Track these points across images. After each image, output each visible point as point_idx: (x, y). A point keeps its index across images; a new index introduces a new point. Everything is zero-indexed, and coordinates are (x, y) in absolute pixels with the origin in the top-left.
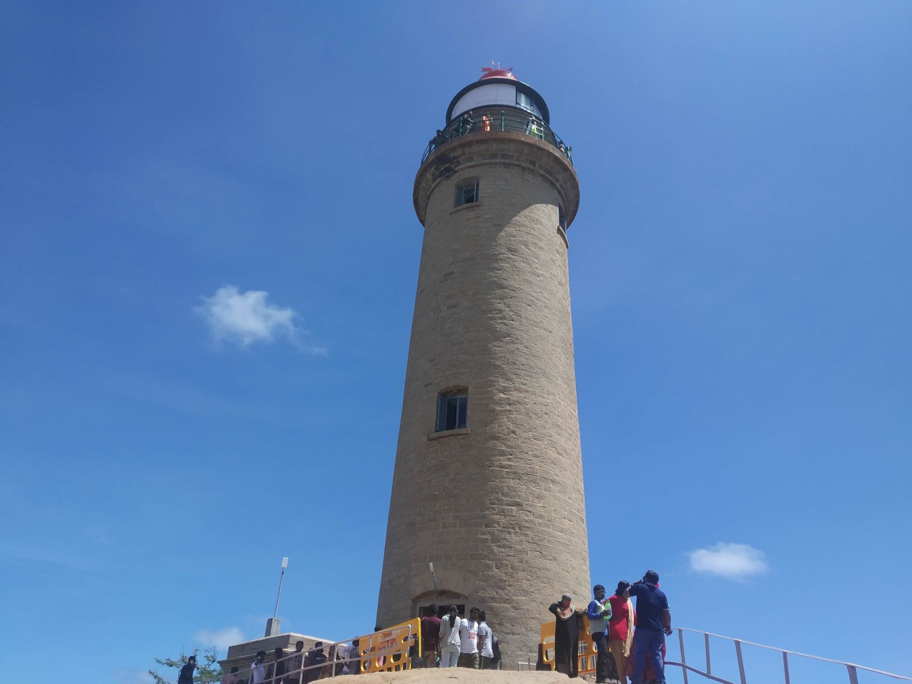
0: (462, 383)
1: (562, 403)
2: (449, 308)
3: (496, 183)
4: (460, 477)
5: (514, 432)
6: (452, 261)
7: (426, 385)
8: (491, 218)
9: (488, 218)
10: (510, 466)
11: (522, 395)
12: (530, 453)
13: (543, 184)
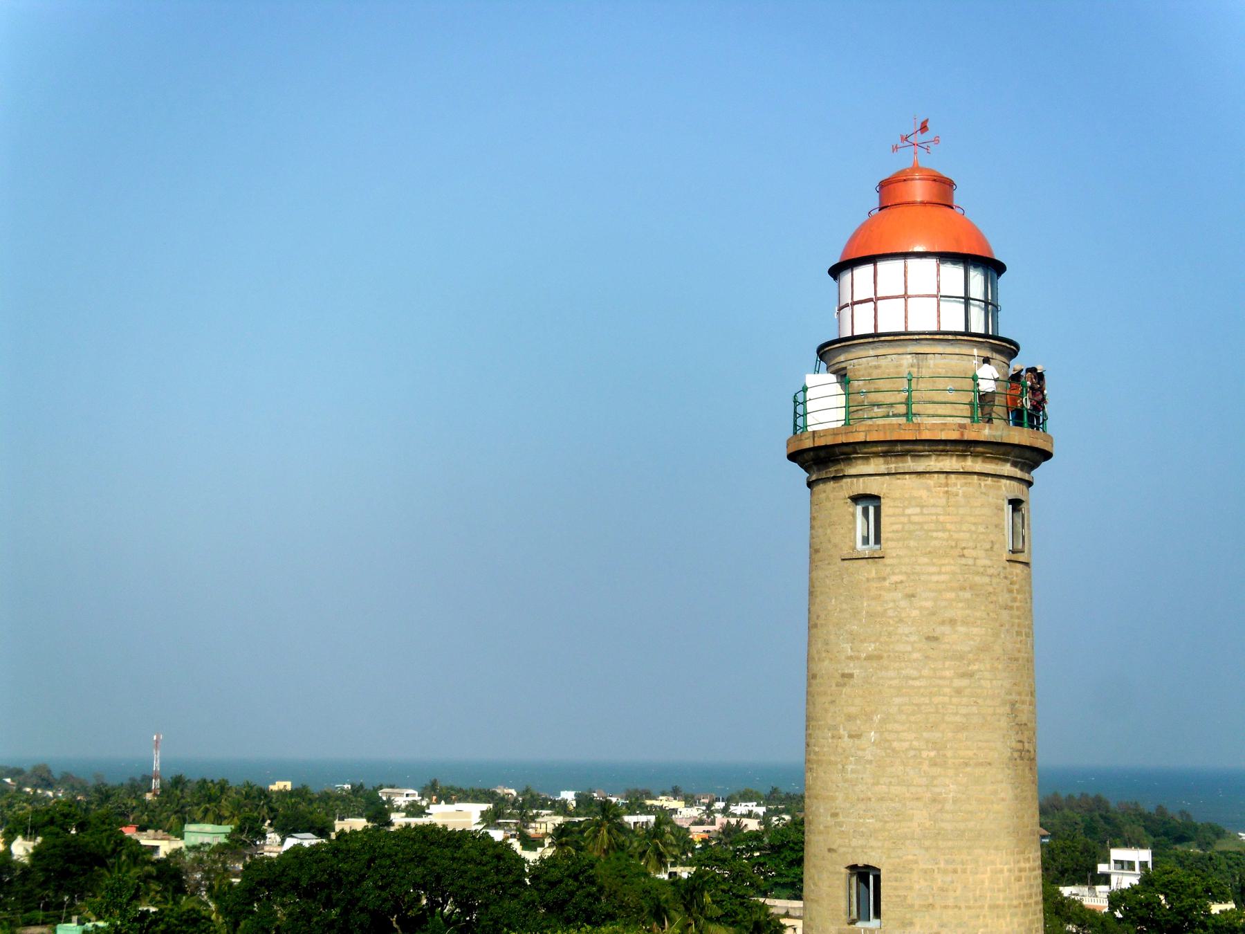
1: (1006, 867)
2: (850, 736)
3: (908, 511)
6: (850, 653)
7: (830, 850)
8: (902, 582)
9: (896, 583)
11: (948, 879)
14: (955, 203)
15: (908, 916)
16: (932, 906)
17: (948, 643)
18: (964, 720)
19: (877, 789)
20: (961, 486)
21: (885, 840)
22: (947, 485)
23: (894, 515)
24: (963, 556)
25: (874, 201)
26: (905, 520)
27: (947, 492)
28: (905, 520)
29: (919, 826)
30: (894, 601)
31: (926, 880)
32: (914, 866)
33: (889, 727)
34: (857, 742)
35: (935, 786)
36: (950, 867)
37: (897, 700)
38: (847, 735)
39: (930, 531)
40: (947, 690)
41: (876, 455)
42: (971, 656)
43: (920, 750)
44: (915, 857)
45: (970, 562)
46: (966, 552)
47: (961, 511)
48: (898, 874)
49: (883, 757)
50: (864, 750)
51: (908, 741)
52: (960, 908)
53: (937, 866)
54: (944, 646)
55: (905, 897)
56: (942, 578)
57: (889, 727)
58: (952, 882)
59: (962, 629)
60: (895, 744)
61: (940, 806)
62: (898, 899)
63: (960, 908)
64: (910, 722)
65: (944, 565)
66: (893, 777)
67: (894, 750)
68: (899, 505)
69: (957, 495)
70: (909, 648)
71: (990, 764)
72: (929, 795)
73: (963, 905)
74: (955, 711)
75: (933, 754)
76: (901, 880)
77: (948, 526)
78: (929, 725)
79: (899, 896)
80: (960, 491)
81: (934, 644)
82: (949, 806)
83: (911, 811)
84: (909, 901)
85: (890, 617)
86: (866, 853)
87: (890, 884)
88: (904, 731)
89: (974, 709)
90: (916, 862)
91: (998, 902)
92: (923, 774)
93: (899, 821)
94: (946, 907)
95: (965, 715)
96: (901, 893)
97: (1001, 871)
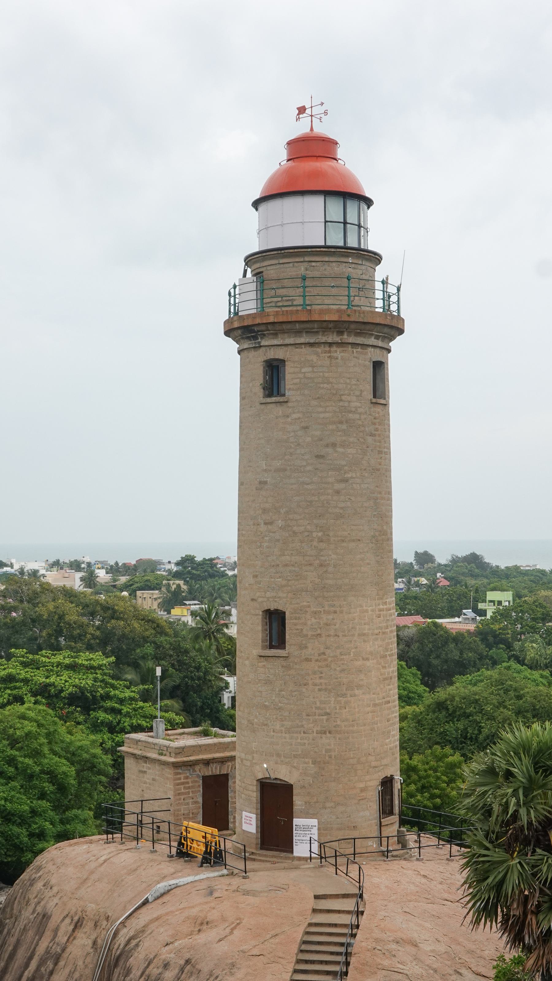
0: (280, 608)
2: (266, 524)
4: (283, 693)
5: (324, 654)
8: (299, 418)
9: (296, 419)
10: (321, 684)
11: (331, 617)
12: (338, 669)
13: (353, 351)
14: (339, 156)
15: (304, 642)
16: (320, 635)
17: (331, 460)
18: (341, 511)
19: (283, 558)
20: (340, 353)
21: (289, 592)
22: (330, 352)
23: (294, 373)
24: (341, 400)
25: (283, 155)
26: (301, 376)
27: (329, 357)
28: (301, 376)
29: (311, 582)
30: (294, 431)
31: (315, 618)
32: (308, 609)
33: (291, 516)
34: (270, 527)
35: (322, 556)
36: (332, 609)
37: (296, 498)
38: (263, 523)
39: (319, 383)
40: (330, 491)
41: (283, 332)
42: (346, 468)
43: (311, 532)
44: (308, 604)
45: (346, 404)
46: (343, 398)
47: (340, 370)
48: (297, 615)
49: (287, 537)
50: (274, 532)
51: (304, 526)
52: (339, 636)
53: (323, 609)
54: (328, 462)
55: (302, 630)
56: (327, 415)
57: (291, 516)
58: (333, 619)
59: (340, 450)
60: (295, 528)
61: (325, 569)
62: (297, 631)
63: (339, 636)
64: (305, 513)
65: (327, 406)
66: (293, 550)
67: (294, 532)
68: (298, 366)
69: (337, 359)
70: (305, 464)
71: (359, 540)
72: (318, 562)
73: (340, 634)
74: (335, 505)
75: (320, 534)
76: (299, 618)
77: (331, 380)
78: (318, 515)
79: (298, 629)
80: (339, 356)
81: (321, 461)
82: (331, 569)
83: (306, 573)
84: (305, 632)
85: (292, 443)
86: (276, 601)
87: (292, 621)
88: (301, 519)
89: (349, 504)
90: (309, 606)
91: (364, 632)
92: (313, 547)
93: (298, 580)
94: (329, 636)
95: (342, 508)
96: (298, 627)
97: (367, 611)
